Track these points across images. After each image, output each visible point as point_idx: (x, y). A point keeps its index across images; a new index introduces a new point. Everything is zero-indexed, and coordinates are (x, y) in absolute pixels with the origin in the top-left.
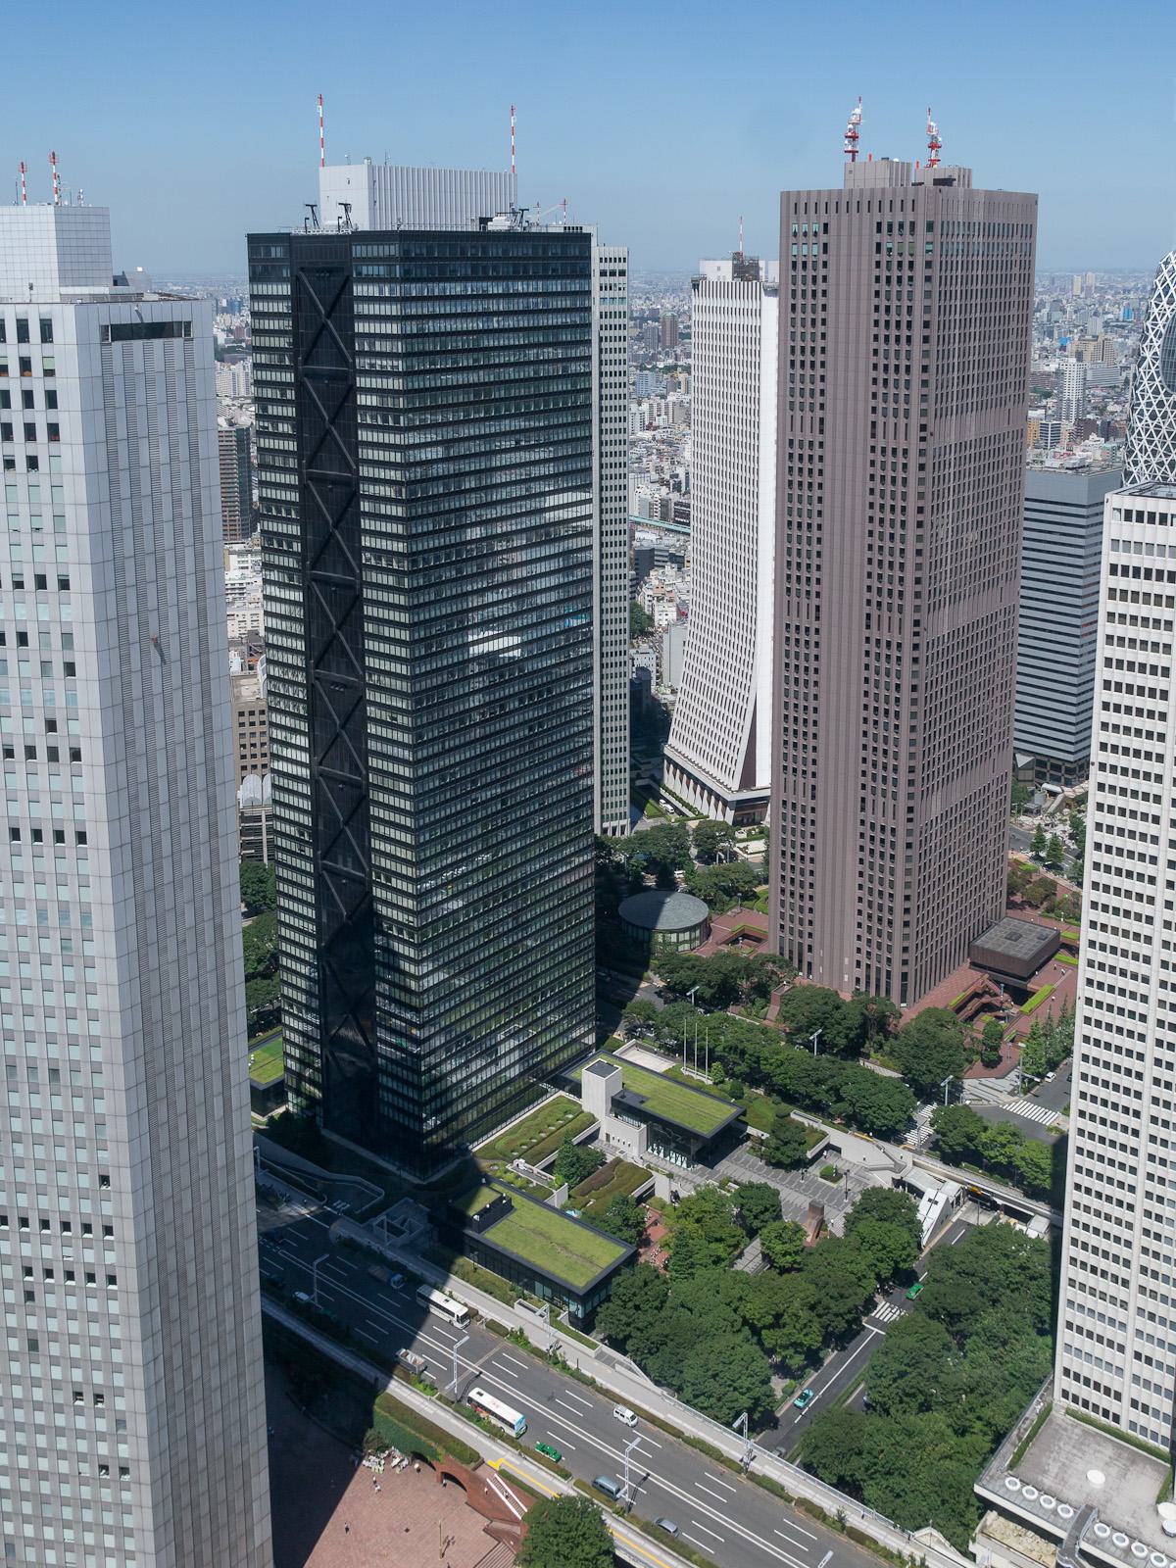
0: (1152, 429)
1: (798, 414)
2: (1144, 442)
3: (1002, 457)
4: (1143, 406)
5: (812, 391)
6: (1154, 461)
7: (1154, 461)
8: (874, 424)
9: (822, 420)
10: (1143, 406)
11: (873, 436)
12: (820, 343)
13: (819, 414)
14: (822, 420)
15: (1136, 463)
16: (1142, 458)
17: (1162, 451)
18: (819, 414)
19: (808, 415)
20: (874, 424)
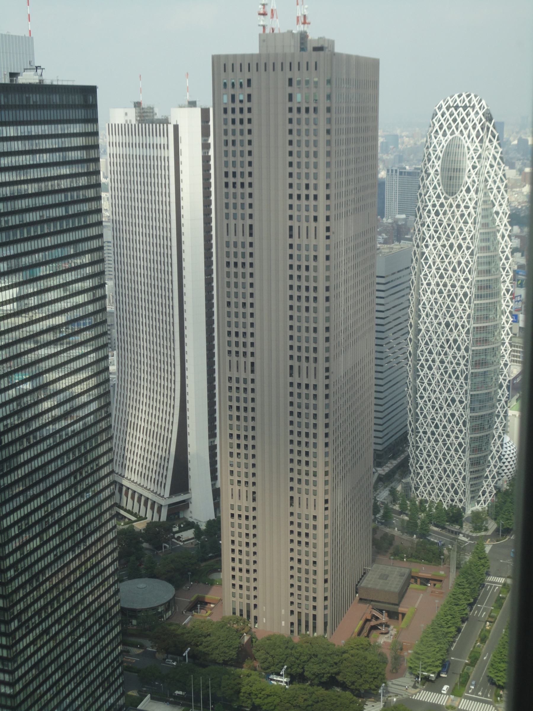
0: (437, 222)
1: (232, 222)
2: (432, 232)
3: (375, 246)
4: (430, 207)
5: (243, 205)
6: (439, 244)
7: (439, 244)
8: (291, 228)
9: (251, 227)
10: (430, 207)
11: (291, 236)
12: (248, 169)
13: (249, 222)
14: (251, 227)
15: (427, 246)
16: (431, 243)
17: (444, 237)
18: (249, 222)
19: (240, 222)
20: (291, 228)
